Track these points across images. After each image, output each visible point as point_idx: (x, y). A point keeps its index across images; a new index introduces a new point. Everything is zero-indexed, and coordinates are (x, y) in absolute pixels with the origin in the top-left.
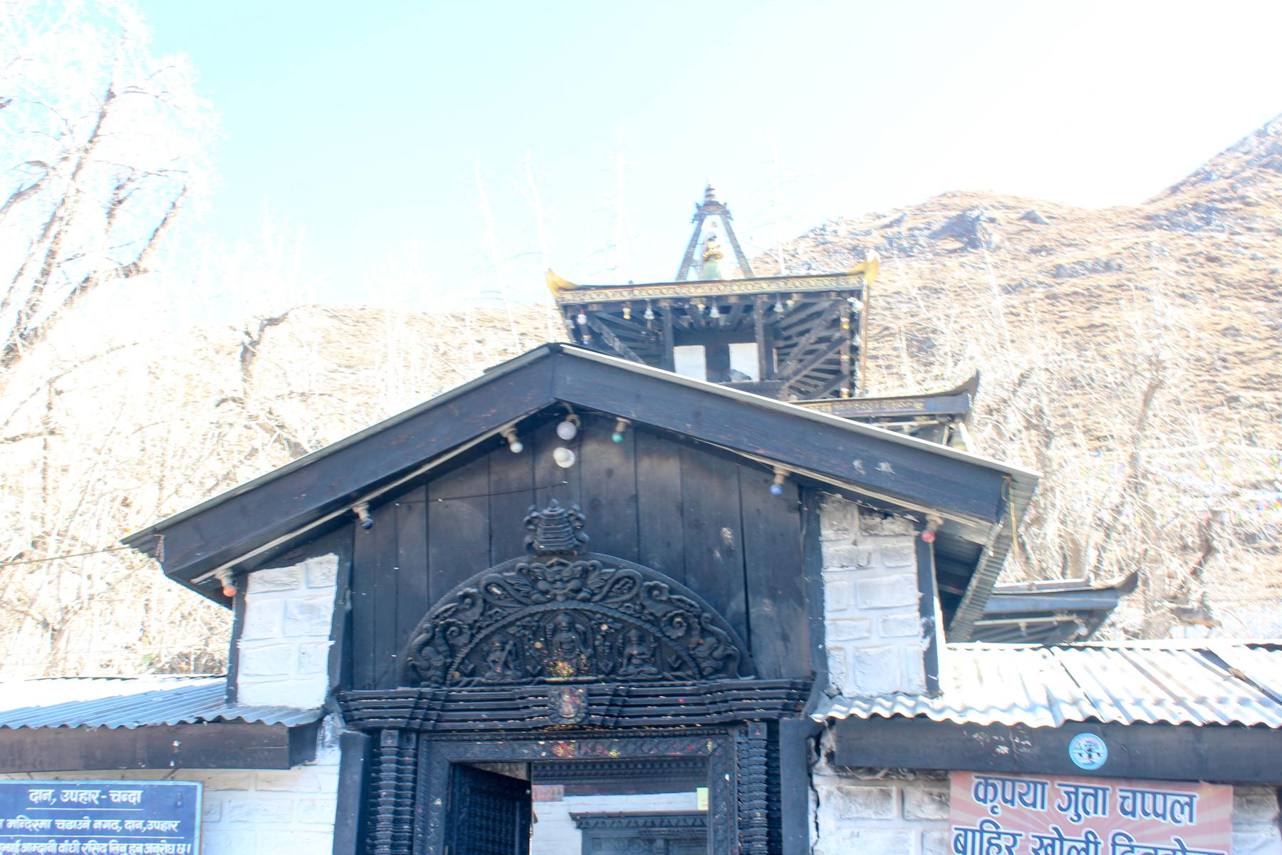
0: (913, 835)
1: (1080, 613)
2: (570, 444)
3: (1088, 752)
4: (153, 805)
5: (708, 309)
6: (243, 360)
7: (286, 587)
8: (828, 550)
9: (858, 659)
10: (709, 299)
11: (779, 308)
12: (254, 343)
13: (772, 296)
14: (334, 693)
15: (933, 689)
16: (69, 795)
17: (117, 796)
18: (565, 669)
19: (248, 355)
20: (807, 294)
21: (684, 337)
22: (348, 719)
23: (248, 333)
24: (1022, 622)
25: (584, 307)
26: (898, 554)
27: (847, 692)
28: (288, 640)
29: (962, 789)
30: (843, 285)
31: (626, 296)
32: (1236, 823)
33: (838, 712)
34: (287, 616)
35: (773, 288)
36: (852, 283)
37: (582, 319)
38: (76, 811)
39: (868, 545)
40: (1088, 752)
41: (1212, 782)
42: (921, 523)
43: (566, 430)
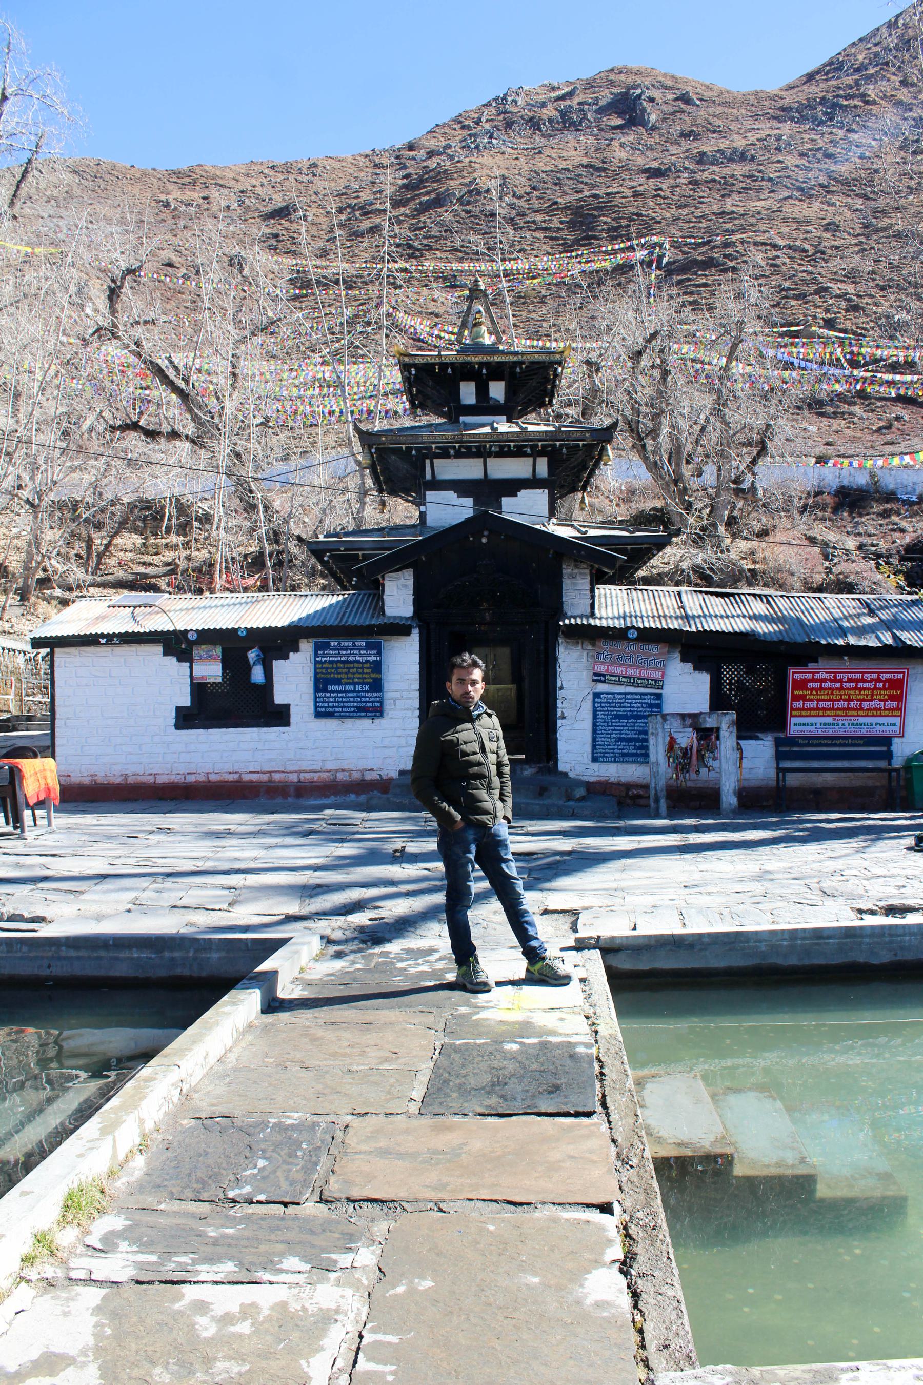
0: (585, 654)
1: (655, 544)
2: (487, 537)
3: (632, 634)
4: (369, 646)
5: (480, 369)
6: (110, 298)
7: (397, 579)
8: (564, 571)
9: (572, 605)
10: (481, 364)
11: (518, 370)
12: (120, 287)
13: (514, 363)
14: (415, 612)
15: (593, 614)
16: (343, 644)
17: (357, 644)
18: (485, 605)
19: (115, 297)
20: (533, 363)
21: (467, 379)
22: (420, 620)
23: (113, 281)
24: (629, 547)
25: (415, 365)
26: (585, 574)
27: (569, 614)
28: (399, 596)
29: (600, 643)
30: (552, 359)
31: (438, 360)
32: (669, 652)
33: (567, 622)
34: (398, 588)
35: (516, 359)
36: (558, 357)
37: (413, 371)
38: (346, 648)
39: (576, 571)
40: (632, 634)
41: (665, 642)
42: (592, 567)
43: (486, 533)
